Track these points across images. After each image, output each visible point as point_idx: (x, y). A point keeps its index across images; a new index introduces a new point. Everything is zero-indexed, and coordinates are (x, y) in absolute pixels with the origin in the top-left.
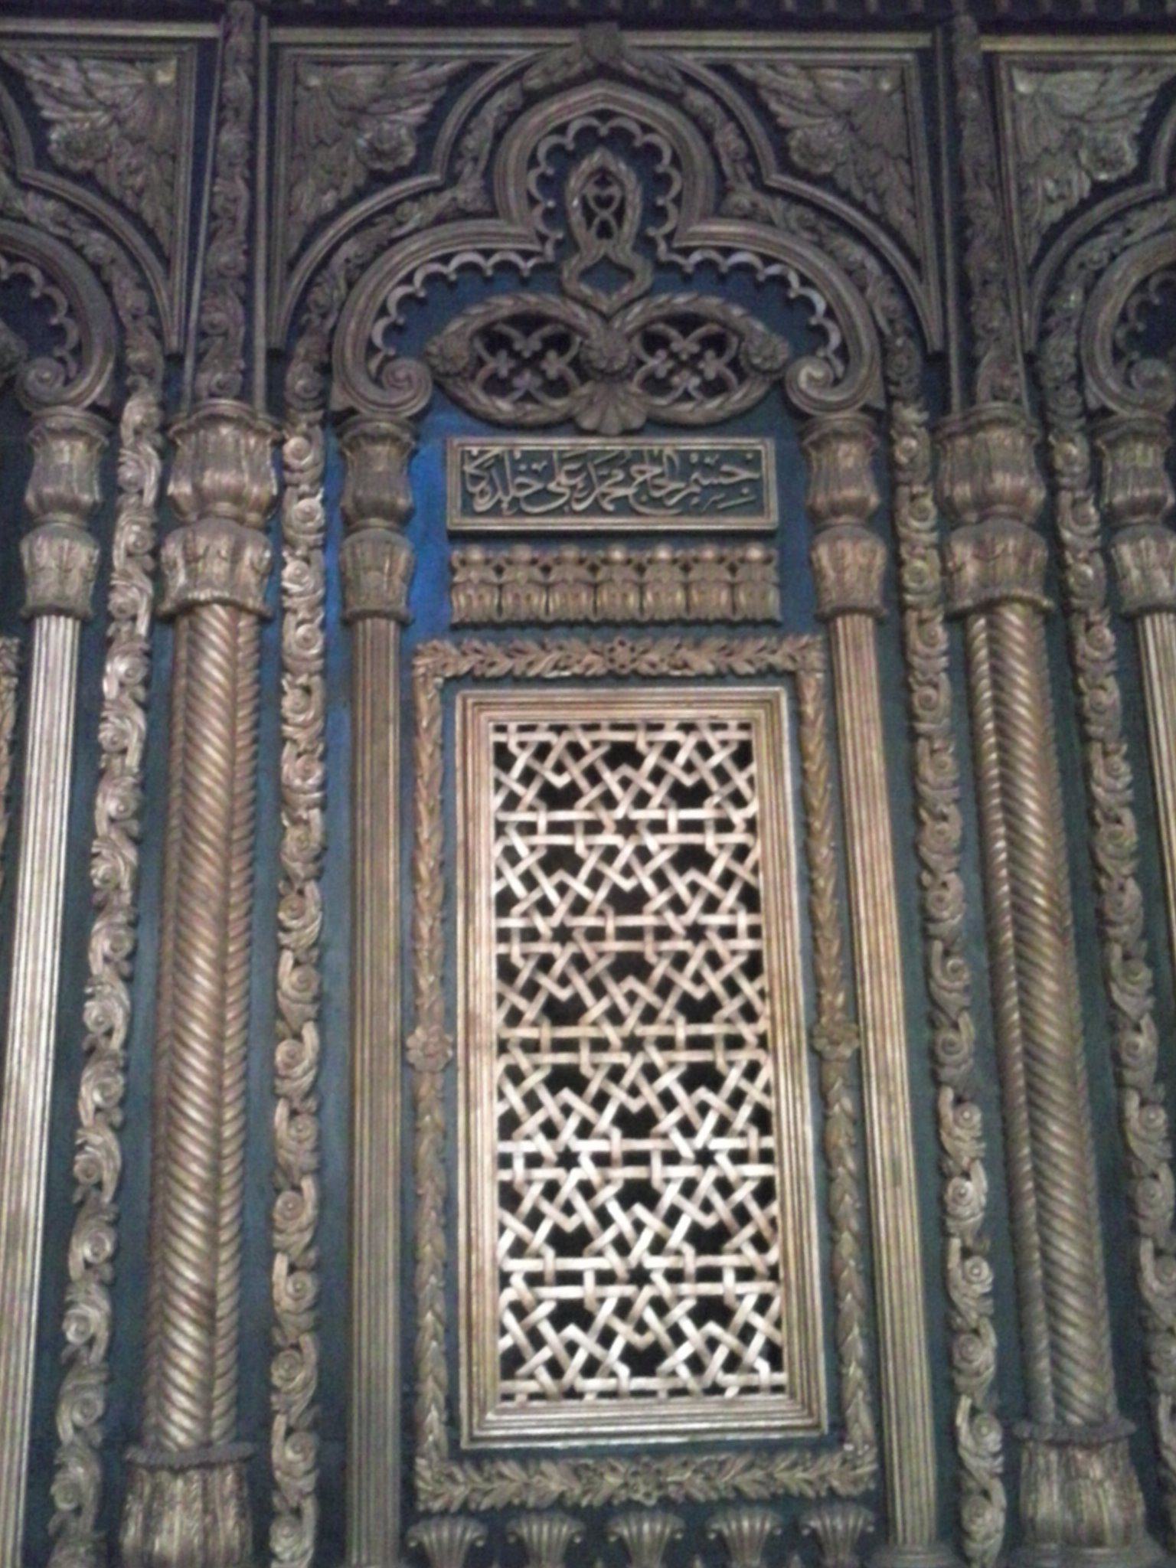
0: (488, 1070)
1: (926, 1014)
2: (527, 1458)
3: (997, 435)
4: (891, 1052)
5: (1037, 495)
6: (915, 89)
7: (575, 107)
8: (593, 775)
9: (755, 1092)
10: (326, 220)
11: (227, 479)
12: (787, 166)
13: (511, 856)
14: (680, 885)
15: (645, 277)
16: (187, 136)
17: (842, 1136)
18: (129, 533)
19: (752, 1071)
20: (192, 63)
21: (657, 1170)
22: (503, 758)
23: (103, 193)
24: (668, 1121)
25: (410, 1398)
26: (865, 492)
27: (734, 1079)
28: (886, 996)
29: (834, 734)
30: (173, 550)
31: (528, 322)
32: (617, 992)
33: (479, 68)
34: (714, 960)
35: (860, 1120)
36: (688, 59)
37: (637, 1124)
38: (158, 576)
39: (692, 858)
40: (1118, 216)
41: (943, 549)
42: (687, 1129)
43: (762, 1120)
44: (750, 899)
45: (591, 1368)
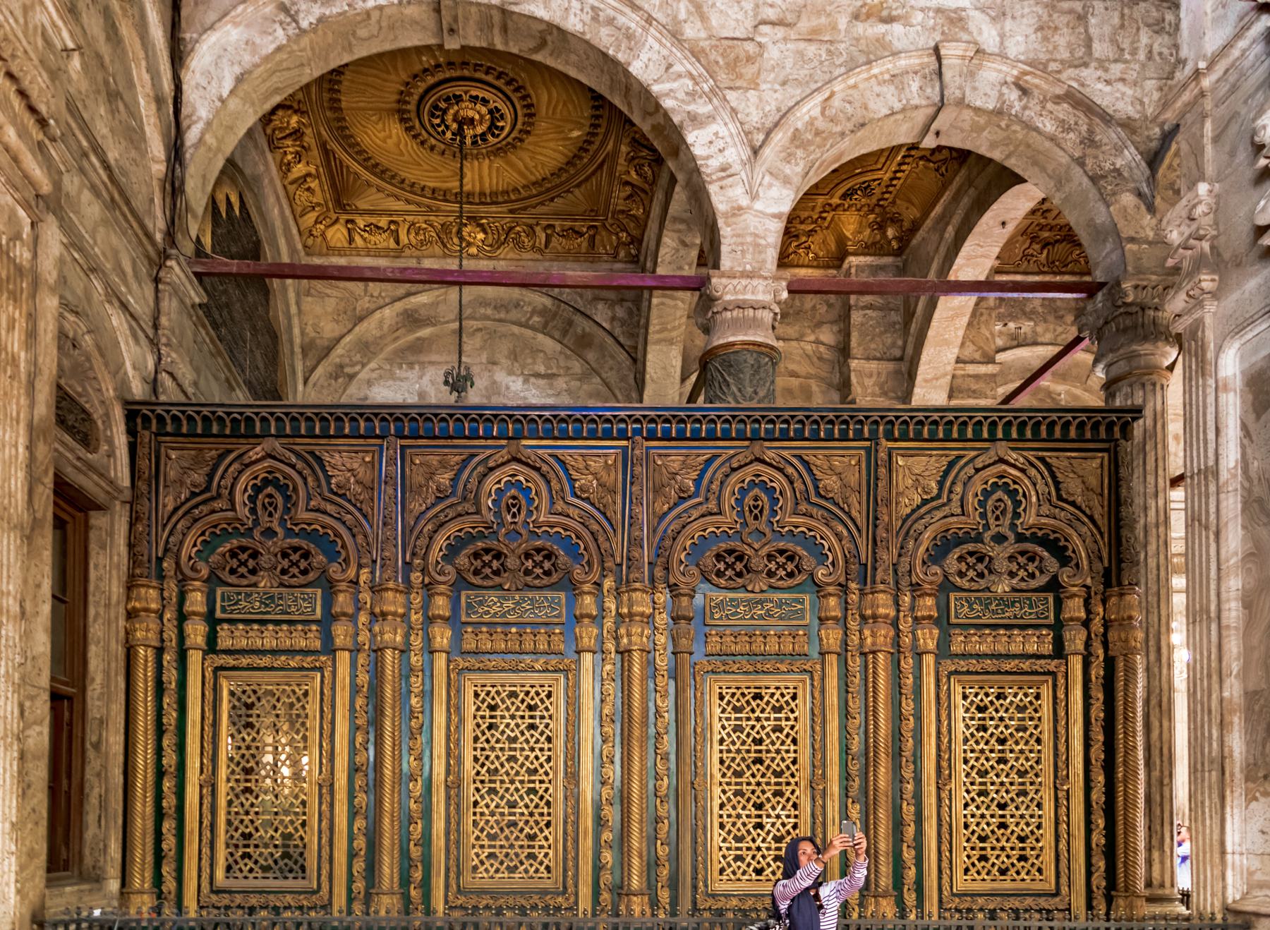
0: (717, 791)
1: (846, 776)
2: (726, 896)
3: (881, 595)
4: (835, 788)
5: (893, 613)
6: (864, 465)
7: (747, 474)
8: (748, 703)
9: (793, 798)
10: (665, 514)
11: (641, 609)
12: (818, 494)
13: (724, 727)
14: (773, 737)
15: (769, 535)
16: (620, 485)
17: (819, 811)
18: (609, 623)
19: (793, 792)
20: (620, 458)
21: (765, 820)
22: (722, 698)
23: (593, 505)
24: (768, 806)
25: (695, 878)
26: (838, 613)
27: (788, 794)
28: (834, 772)
29: (823, 691)
30: (622, 631)
31: (730, 552)
32: (754, 768)
33: (715, 457)
34: (783, 760)
35: (824, 807)
36: (785, 453)
37: (759, 807)
38: (617, 639)
39: (778, 729)
40: (929, 512)
41: (860, 632)
42: (774, 808)
43: (795, 806)
44: (794, 741)
45: (744, 873)
